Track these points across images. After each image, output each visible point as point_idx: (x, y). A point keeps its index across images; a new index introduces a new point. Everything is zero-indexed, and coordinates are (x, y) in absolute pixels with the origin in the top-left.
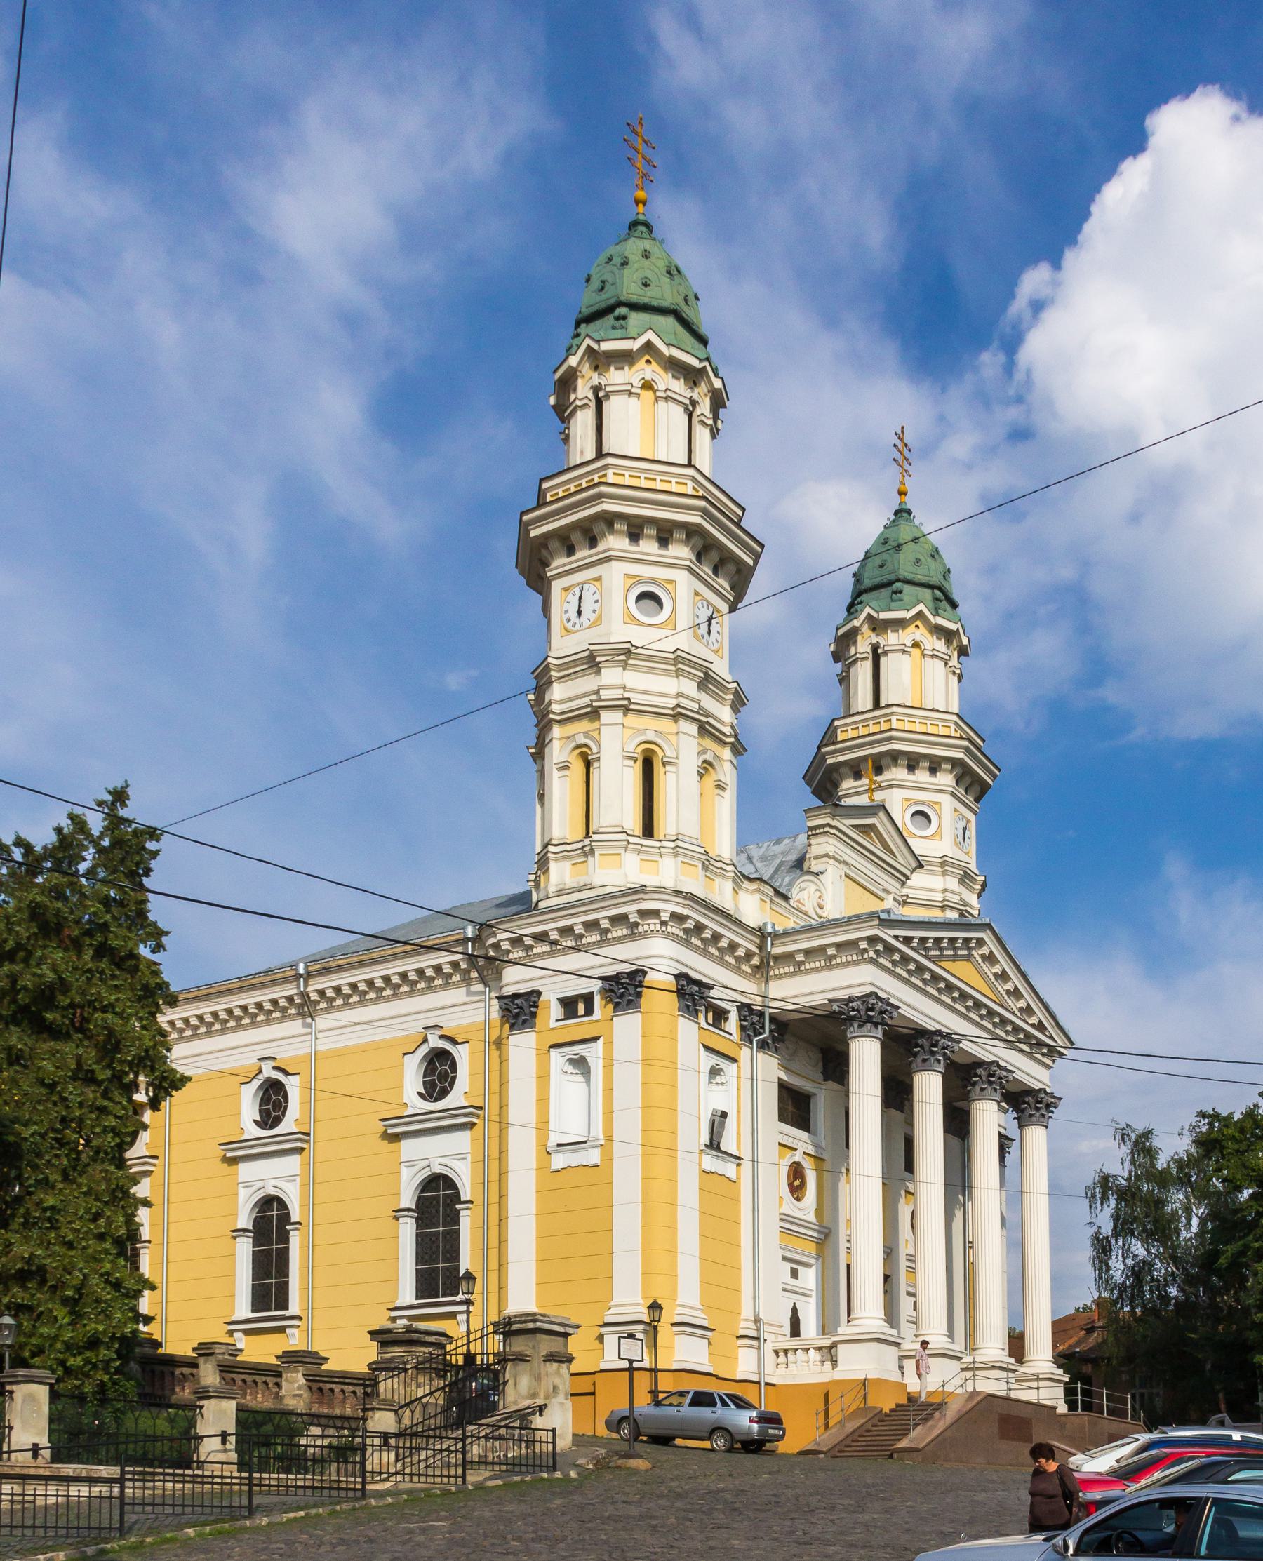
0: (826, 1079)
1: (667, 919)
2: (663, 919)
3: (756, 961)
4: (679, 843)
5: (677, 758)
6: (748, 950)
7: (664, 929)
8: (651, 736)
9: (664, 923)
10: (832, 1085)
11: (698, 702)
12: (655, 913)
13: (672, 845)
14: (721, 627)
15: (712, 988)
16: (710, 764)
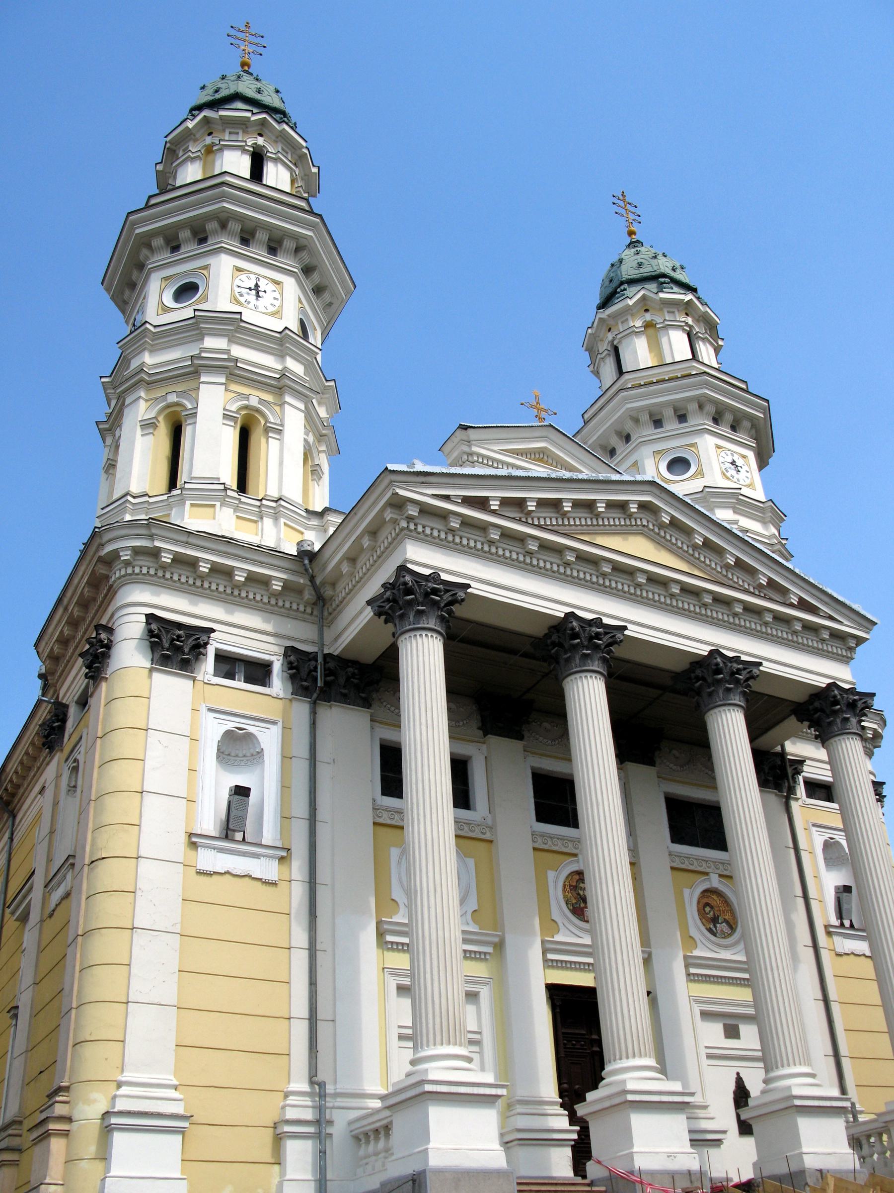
0: (485, 735)
1: (128, 557)
2: (122, 558)
3: (308, 595)
4: (187, 486)
5: (197, 407)
6: (285, 581)
7: (130, 571)
8: (172, 398)
9: (127, 563)
10: (493, 739)
11: (227, 352)
12: (115, 554)
13: (179, 492)
14: (282, 294)
15: (213, 631)
16: (258, 410)
